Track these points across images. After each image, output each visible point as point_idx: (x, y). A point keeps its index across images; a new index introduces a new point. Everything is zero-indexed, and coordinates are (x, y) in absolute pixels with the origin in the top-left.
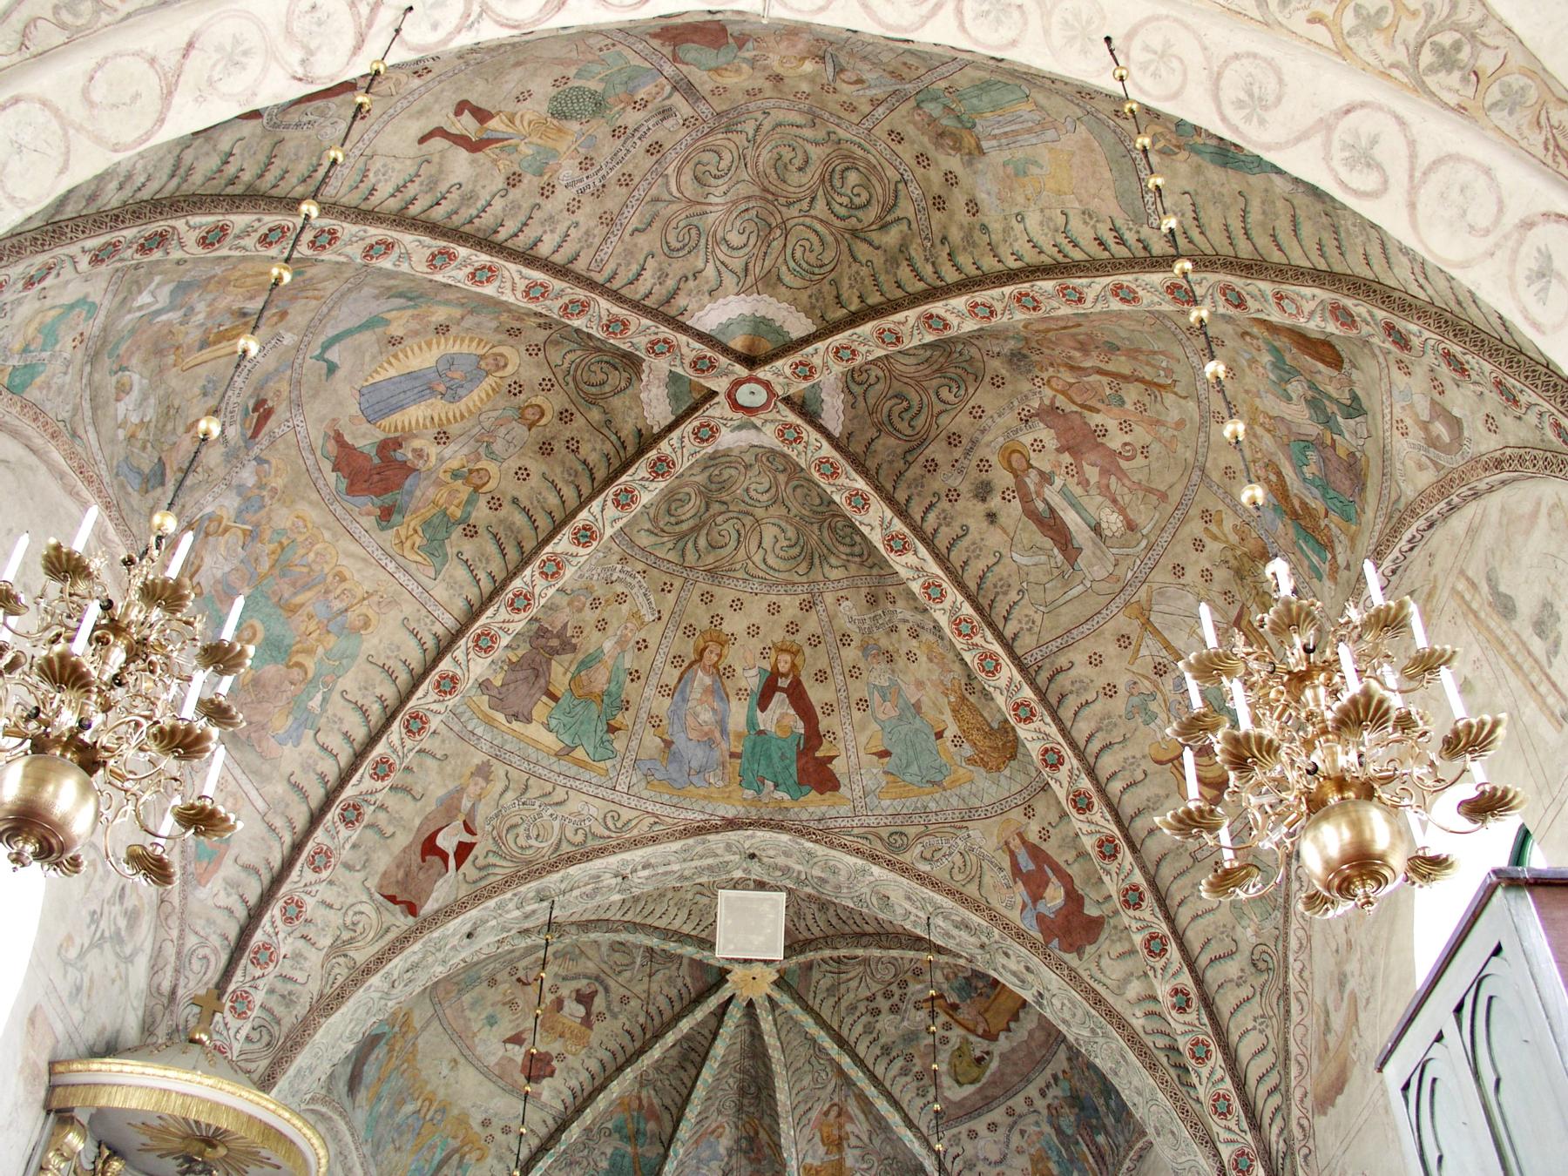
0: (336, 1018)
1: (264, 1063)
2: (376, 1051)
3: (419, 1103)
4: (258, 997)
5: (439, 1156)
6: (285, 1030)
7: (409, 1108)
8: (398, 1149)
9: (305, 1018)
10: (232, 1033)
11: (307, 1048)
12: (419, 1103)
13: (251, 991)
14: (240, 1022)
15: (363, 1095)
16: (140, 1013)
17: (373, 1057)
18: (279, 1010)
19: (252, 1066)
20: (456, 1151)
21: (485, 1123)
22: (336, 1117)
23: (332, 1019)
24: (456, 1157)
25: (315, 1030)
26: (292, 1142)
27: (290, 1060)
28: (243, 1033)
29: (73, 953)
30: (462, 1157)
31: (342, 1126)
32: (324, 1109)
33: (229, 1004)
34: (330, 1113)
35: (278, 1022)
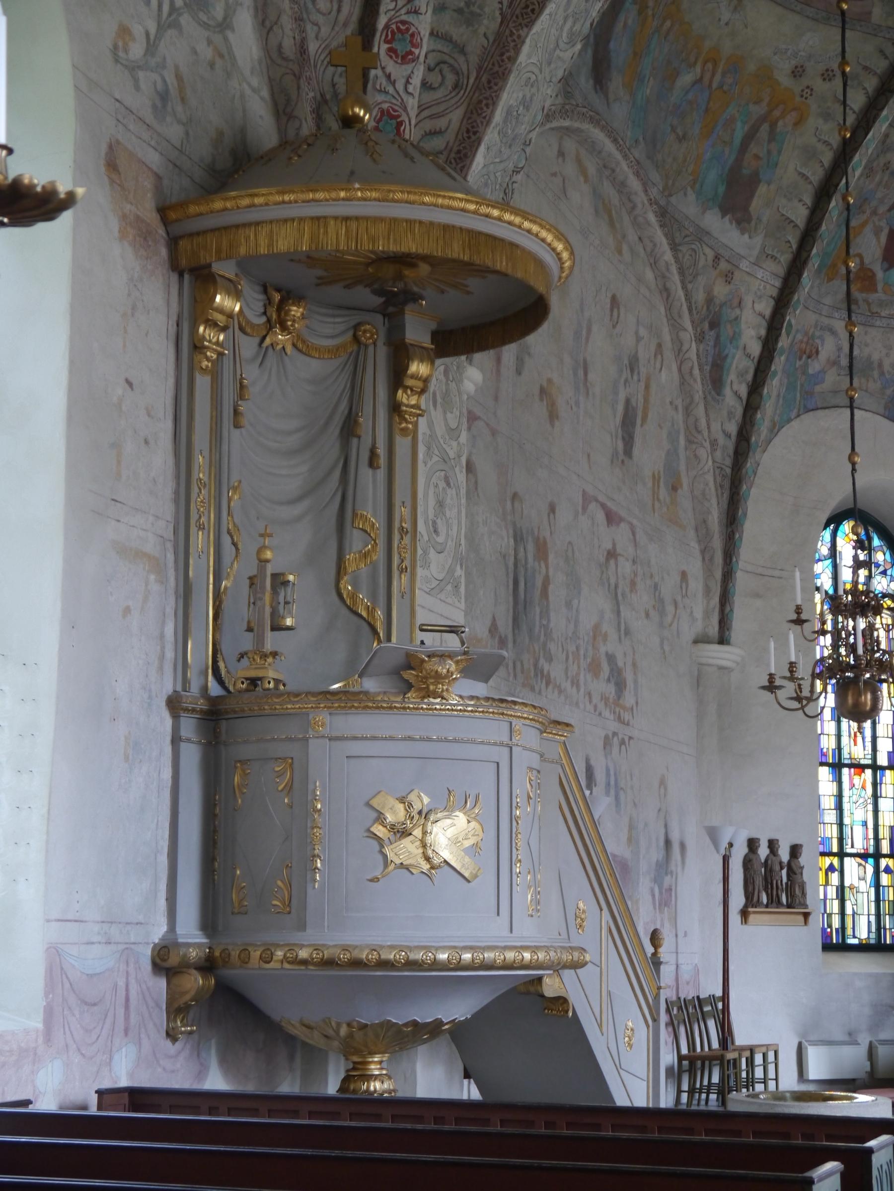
0: (543, 22)
1: (456, 116)
2: (622, 18)
3: (698, 69)
4: (424, 24)
5: (740, 132)
6: (474, 59)
7: (687, 78)
8: (682, 139)
9: (499, 35)
10: (400, 86)
11: (512, 79)
12: (698, 69)
13: (410, 18)
14: (408, 68)
15: (616, 83)
16: (265, 93)
17: (619, 26)
18: (459, 33)
19: (441, 123)
20: (763, 119)
21: (797, 72)
22: (585, 126)
23: (537, 28)
24: (765, 127)
25: (517, 50)
26: (513, 246)
27: (492, 102)
28: (416, 81)
29: (137, 50)
30: (773, 125)
31: (598, 134)
32: (567, 123)
33: (385, 47)
34: (576, 125)
35: (462, 51)
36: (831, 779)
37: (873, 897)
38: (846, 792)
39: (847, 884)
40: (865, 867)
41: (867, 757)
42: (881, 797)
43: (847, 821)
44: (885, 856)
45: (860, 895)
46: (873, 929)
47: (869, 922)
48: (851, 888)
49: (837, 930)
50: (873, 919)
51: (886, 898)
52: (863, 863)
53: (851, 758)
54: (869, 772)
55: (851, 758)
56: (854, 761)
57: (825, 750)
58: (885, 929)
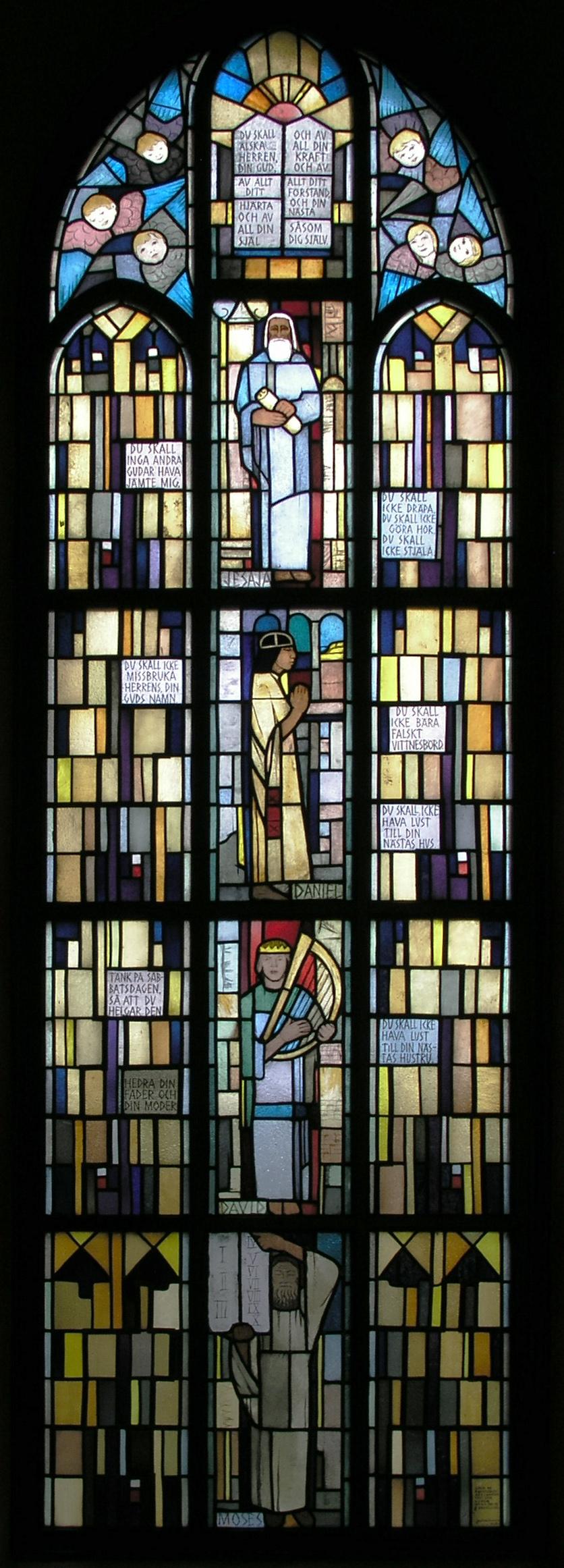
36: (158, 960)
37: (333, 1367)
38: (228, 1007)
39: (220, 1319)
40: (302, 1266)
41: (321, 874)
42: (384, 1012)
43: (228, 1103)
44: (394, 1224)
45: (275, 1364)
46: (333, 1479)
47: (315, 1458)
48: (240, 1334)
49: (171, 1484)
50: (330, 1443)
51: (394, 1370)
52: (296, 1250)
53: (249, 883)
54: (331, 934)
55: (249, 883)
56: (262, 893)
57: (136, 859)
58: (385, 1474)
